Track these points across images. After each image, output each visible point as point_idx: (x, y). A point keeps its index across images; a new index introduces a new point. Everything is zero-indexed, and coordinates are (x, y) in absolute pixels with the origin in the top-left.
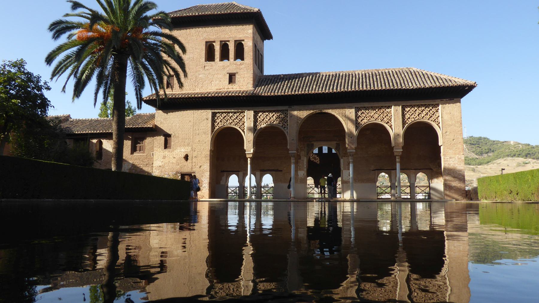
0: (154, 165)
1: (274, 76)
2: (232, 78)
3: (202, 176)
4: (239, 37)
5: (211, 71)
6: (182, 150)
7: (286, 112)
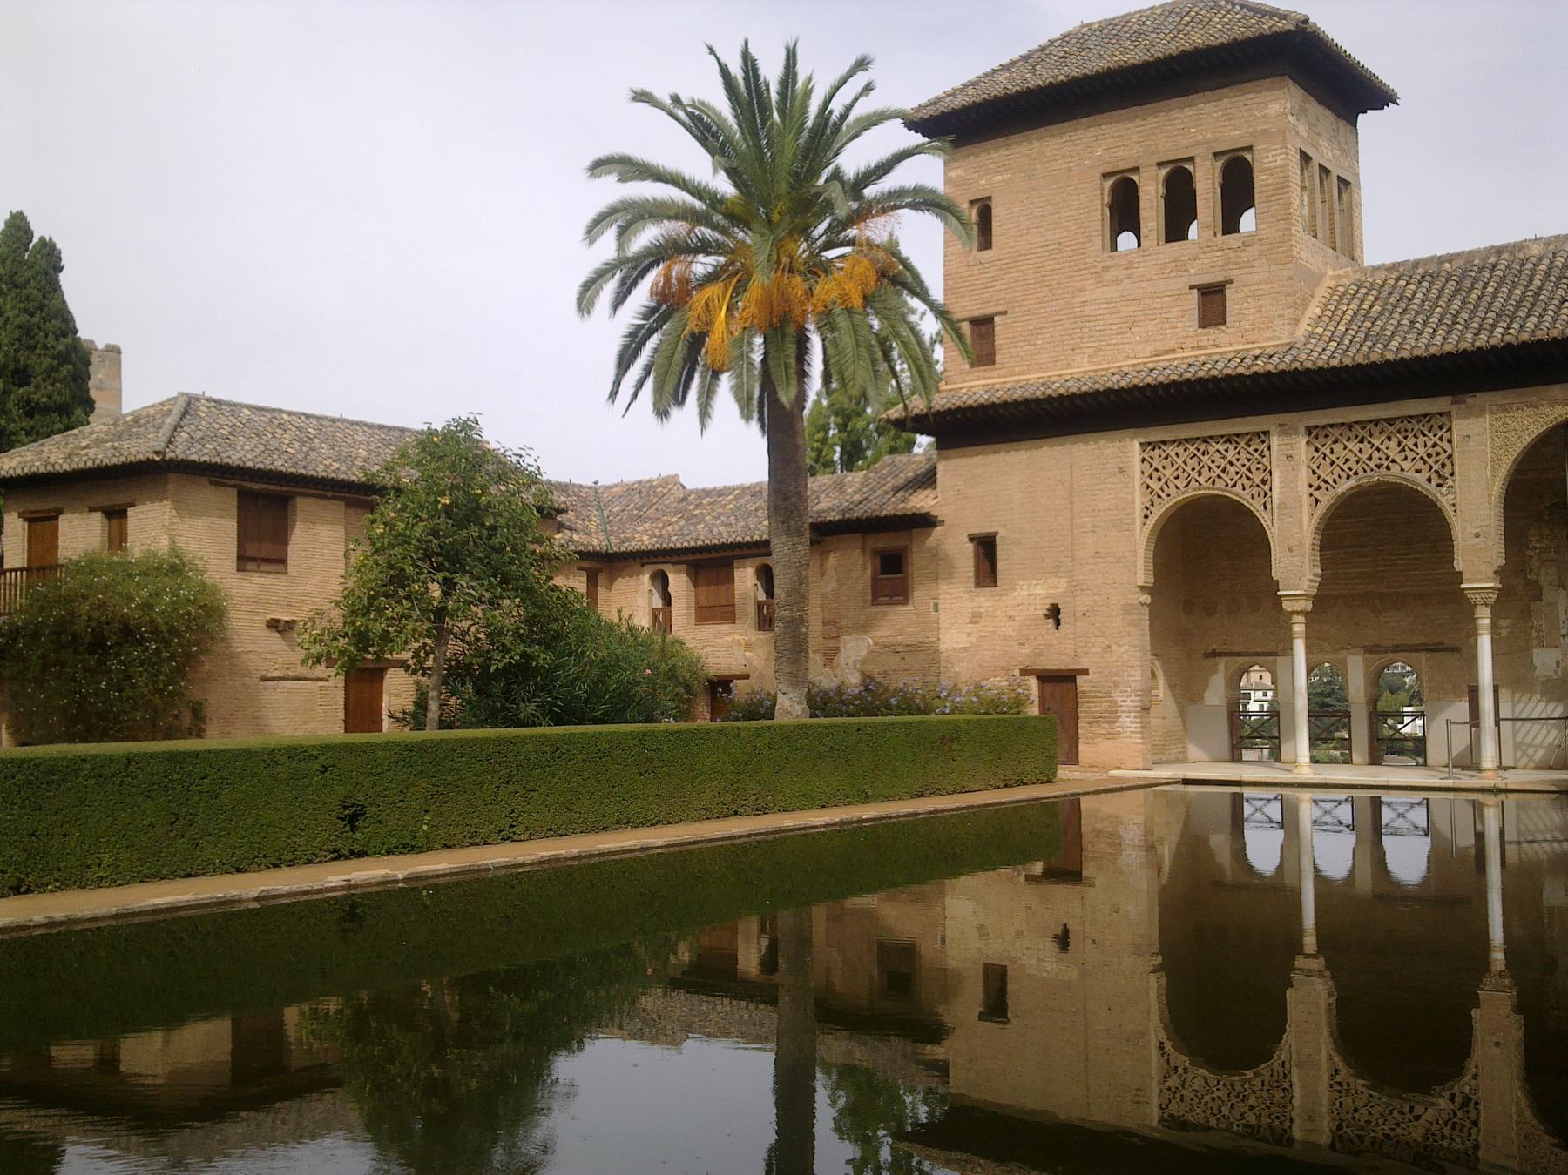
2: (1212, 301)
3: (1116, 685)
4: (1232, 136)
6: (1038, 590)
7: (1444, 419)
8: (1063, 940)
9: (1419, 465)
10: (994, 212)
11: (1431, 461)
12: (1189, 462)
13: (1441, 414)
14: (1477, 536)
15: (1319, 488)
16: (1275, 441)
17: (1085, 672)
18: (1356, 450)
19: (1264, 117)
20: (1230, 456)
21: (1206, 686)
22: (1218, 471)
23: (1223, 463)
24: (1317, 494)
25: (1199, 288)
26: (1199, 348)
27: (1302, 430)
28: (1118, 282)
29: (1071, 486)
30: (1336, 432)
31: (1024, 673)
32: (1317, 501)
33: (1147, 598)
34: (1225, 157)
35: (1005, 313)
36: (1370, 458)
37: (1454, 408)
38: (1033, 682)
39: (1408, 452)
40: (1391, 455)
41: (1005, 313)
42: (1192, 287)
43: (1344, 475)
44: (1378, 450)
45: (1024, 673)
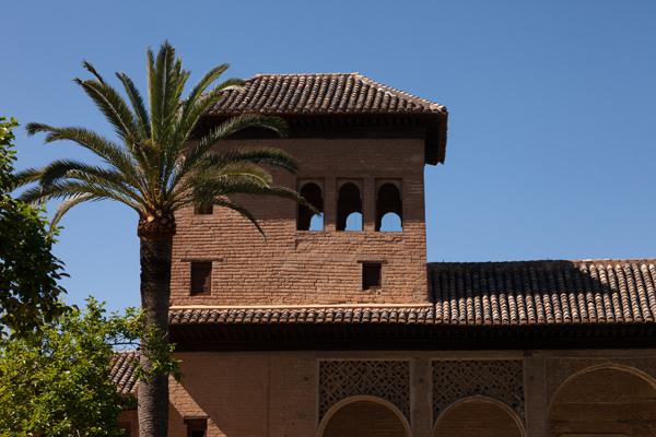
1: (466, 265)
2: (371, 275)
5: (313, 253)
26: (362, 302)
35: (221, 260)
42: (359, 262)
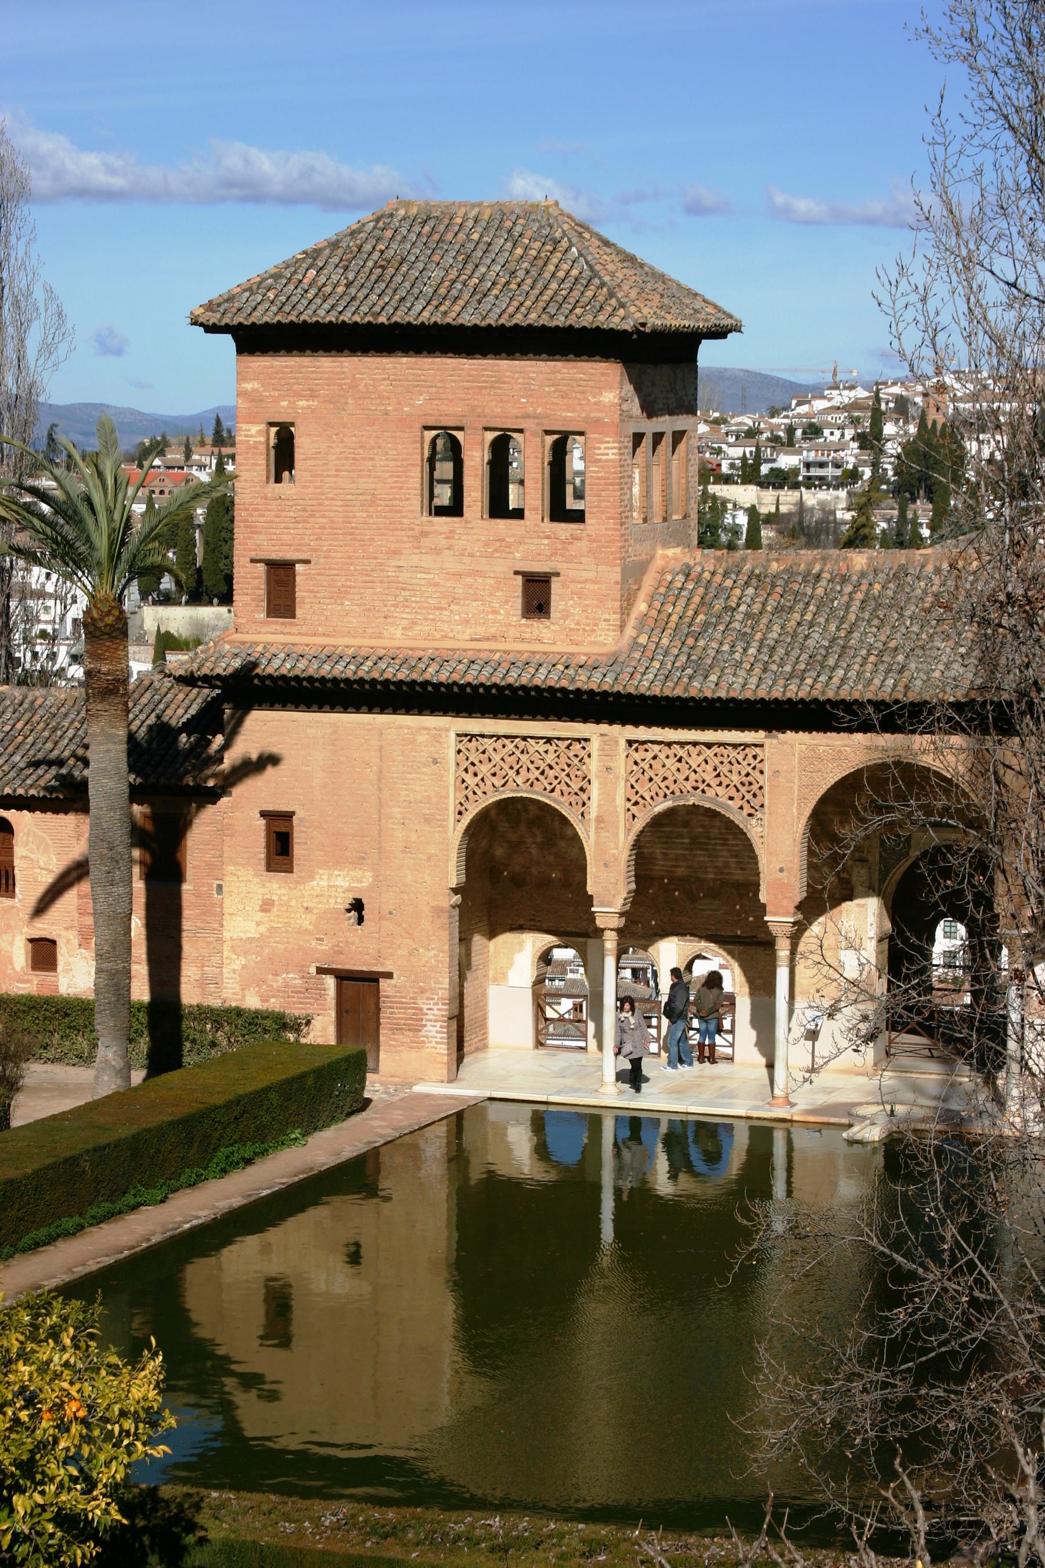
0: (227, 935)
2: (537, 594)
3: (423, 991)
6: (340, 882)
7: (758, 750)
8: (355, 1257)
9: (732, 792)
10: (298, 442)
11: (743, 790)
12: (508, 759)
13: (756, 745)
14: (781, 870)
15: (636, 803)
16: (594, 746)
17: (389, 975)
18: (674, 769)
19: (596, 404)
20: (550, 758)
21: (511, 964)
22: (537, 773)
23: (543, 766)
24: (634, 810)
25: (524, 574)
26: (523, 640)
27: (623, 744)
28: (437, 552)
29: (380, 771)
30: (656, 748)
31: (321, 971)
32: (634, 816)
33: (457, 899)
34: (556, 437)
35: (307, 562)
36: (687, 779)
37: (767, 742)
38: (330, 982)
39: (722, 778)
40: (707, 779)
41: (307, 562)
42: (516, 573)
43: (661, 794)
44: (695, 772)
45: (321, 971)
